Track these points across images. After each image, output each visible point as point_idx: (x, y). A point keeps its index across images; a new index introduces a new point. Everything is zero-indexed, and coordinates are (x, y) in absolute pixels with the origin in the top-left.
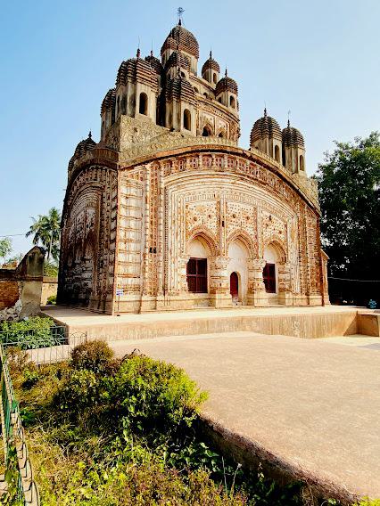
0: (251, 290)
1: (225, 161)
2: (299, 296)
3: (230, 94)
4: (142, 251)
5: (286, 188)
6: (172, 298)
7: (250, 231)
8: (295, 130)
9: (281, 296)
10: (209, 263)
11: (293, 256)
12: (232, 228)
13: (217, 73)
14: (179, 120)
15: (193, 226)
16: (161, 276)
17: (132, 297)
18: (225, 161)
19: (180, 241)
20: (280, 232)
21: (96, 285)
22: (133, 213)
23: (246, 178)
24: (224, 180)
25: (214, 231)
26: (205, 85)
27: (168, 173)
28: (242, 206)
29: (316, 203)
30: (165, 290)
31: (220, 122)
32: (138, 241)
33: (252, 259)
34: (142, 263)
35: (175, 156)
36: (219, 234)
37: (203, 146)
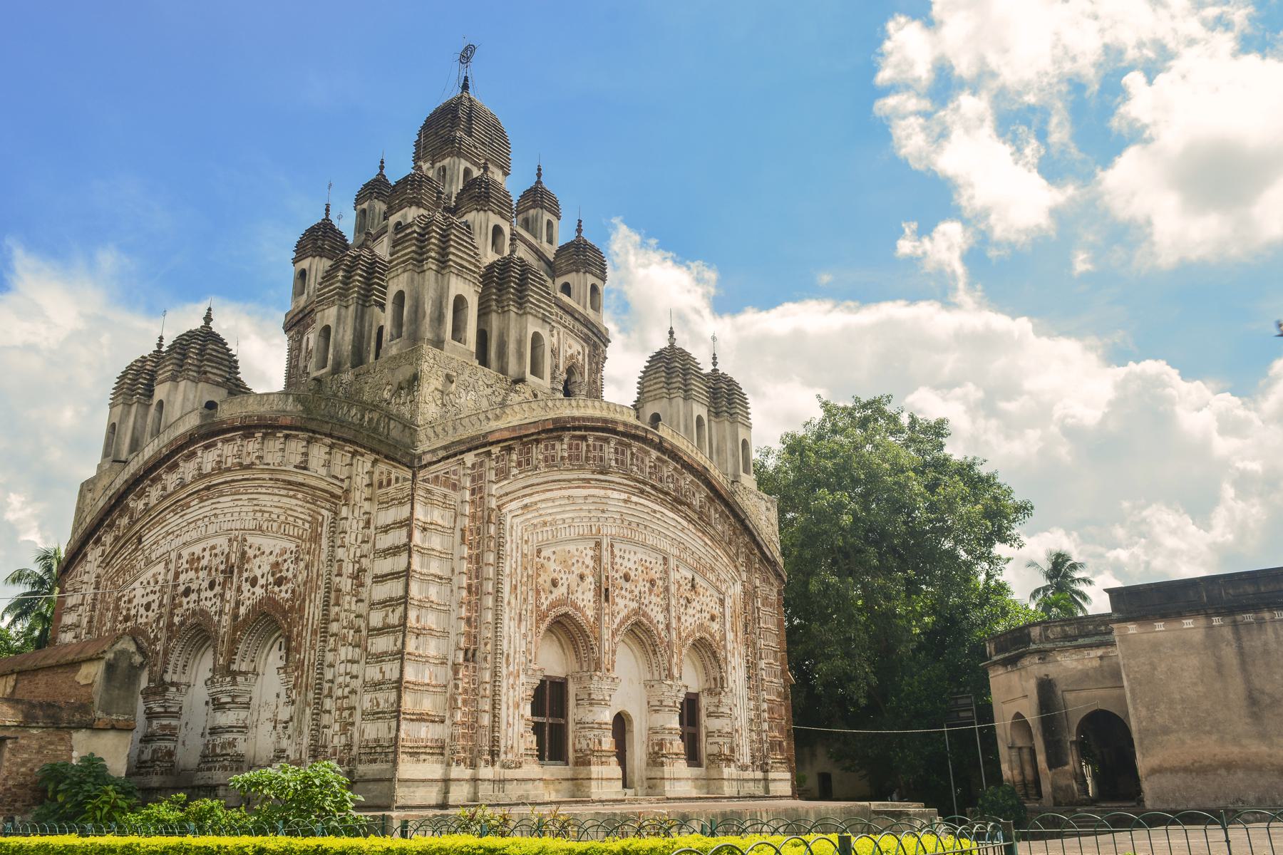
0: (656, 758)
1: (609, 451)
2: (749, 774)
3: (591, 279)
4: (451, 658)
6: (509, 774)
7: (658, 616)
8: (730, 382)
9: (714, 774)
10: (572, 688)
11: (736, 676)
12: (623, 605)
13: (553, 219)
14: (520, 356)
16: (486, 720)
17: (432, 769)
18: (609, 451)
19: (525, 636)
20: (713, 618)
21: (306, 741)
22: (435, 567)
23: (648, 489)
24: (609, 492)
25: (590, 613)
26: (531, 246)
27: (503, 474)
29: (775, 551)
30: (494, 754)
31: (571, 341)
32: (445, 634)
33: (661, 681)
34: (452, 684)
35: (520, 438)
36: (598, 618)
37: (574, 419)
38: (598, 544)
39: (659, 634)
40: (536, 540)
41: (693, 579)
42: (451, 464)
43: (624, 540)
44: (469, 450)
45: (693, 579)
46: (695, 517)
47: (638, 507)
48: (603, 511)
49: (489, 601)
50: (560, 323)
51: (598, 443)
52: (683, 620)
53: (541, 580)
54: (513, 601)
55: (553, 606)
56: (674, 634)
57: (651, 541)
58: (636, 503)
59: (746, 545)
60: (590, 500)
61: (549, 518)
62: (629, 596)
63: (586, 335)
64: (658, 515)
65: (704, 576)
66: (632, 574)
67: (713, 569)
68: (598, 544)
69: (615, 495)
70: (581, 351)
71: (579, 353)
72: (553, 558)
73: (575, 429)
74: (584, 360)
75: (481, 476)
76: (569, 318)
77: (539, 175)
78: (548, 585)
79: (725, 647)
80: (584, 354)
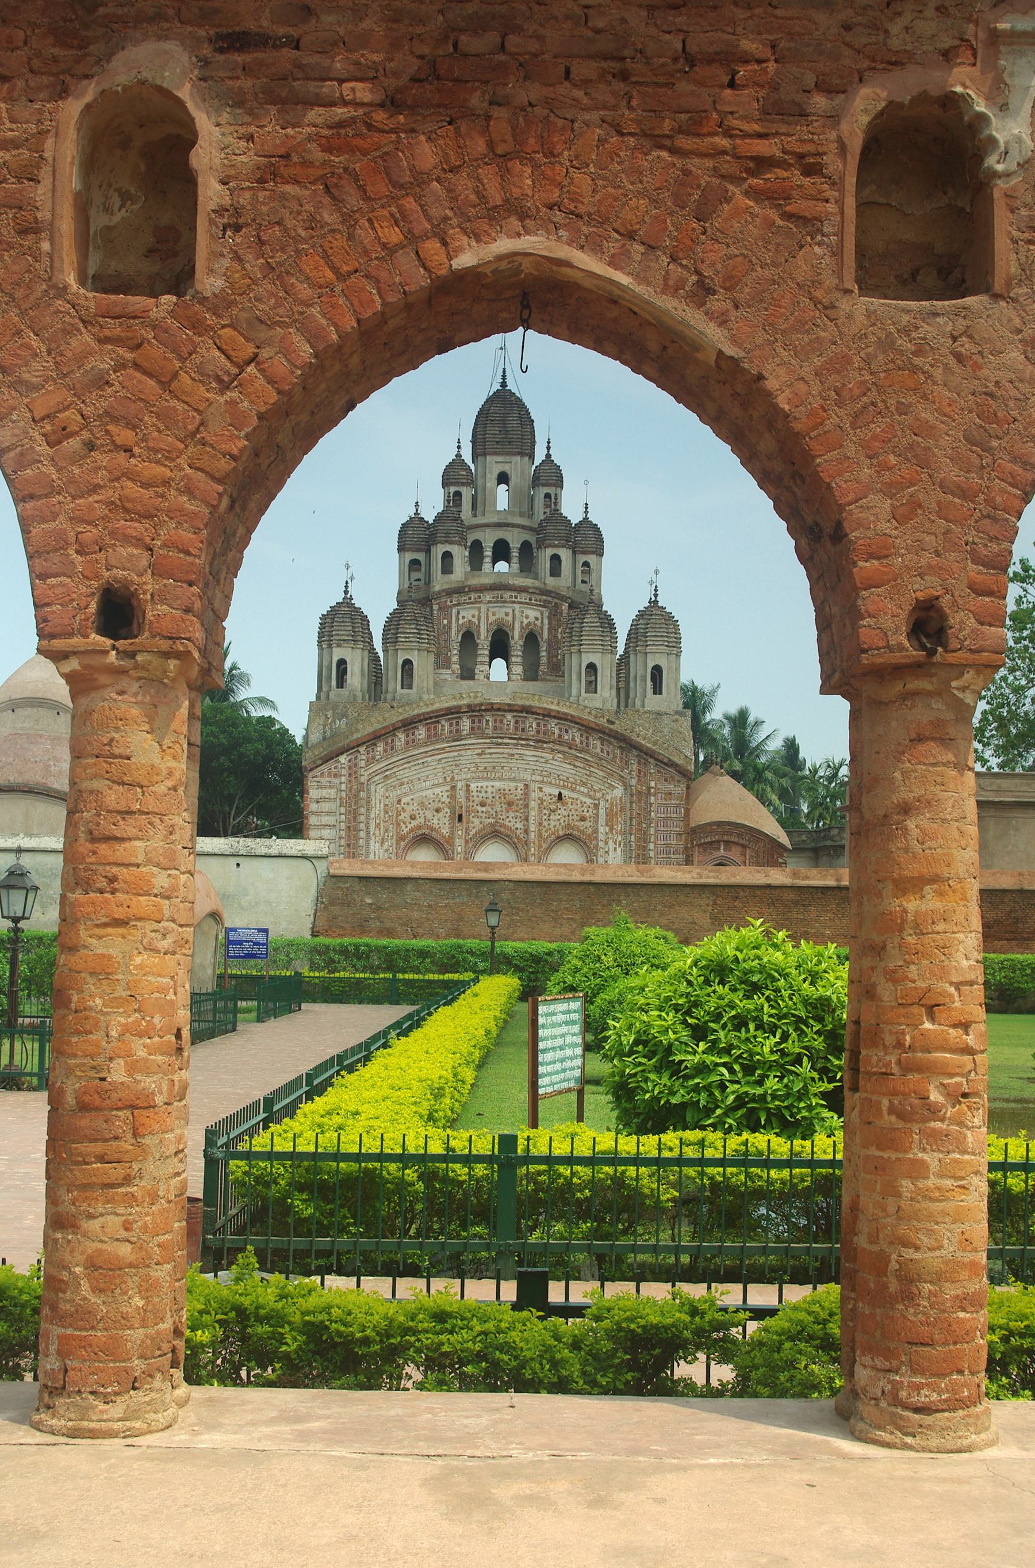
1: (466, 724)
5: (600, 738)
15: (409, 826)
18: (466, 724)
19: (387, 851)
20: (583, 819)
24: (463, 753)
27: (370, 761)
28: (498, 784)
36: (452, 833)
38: (453, 788)
39: (518, 838)
40: (394, 794)
41: (560, 794)
42: (331, 764)
43: (478, 779)
44: (342, 753)
45: (560, 794)
46: (566, 749)
47: (494, 756)
48: (456, 765)
49: (362, 834)
50: (514, 602)
51: (454, 722)
52: (545, 823)
53: (400, 818)
54: (377, 833)
55: (411, 830)
56: (532, 835)
57: (507, 774)
58: (491, 754)
59: (638, 756)
60: (444, 761)
61: (406, 780)
62: (484, 815)
63: (545, 601)
64: (517, 756)
65: (573, 790)
66: (489, 801)
67: (584, 784)
68: (453, 788)
69: (469, 752)
70: (539, 616)
71: (537, 619)
72: (411, 803)
73: (426, 719)
74: (542, 622)
75: (356, 765)
76: (524, 595)
77: (548, 448)
78: (408, 819)
79: (596, 838)
80: (542, 619)
